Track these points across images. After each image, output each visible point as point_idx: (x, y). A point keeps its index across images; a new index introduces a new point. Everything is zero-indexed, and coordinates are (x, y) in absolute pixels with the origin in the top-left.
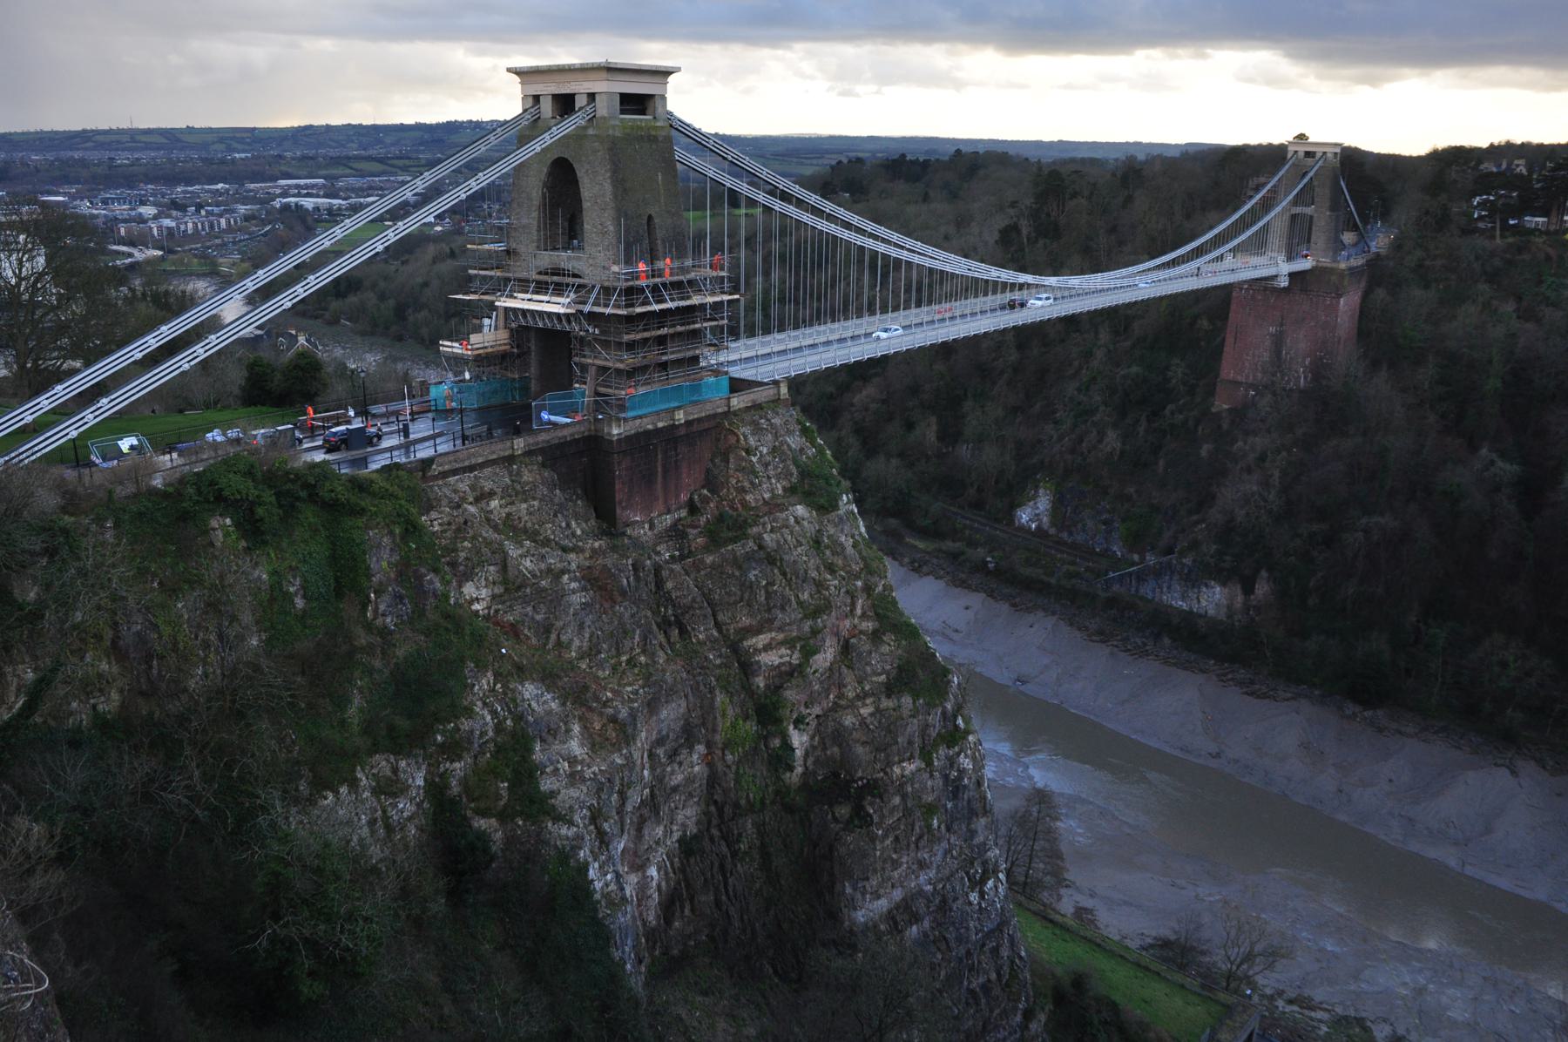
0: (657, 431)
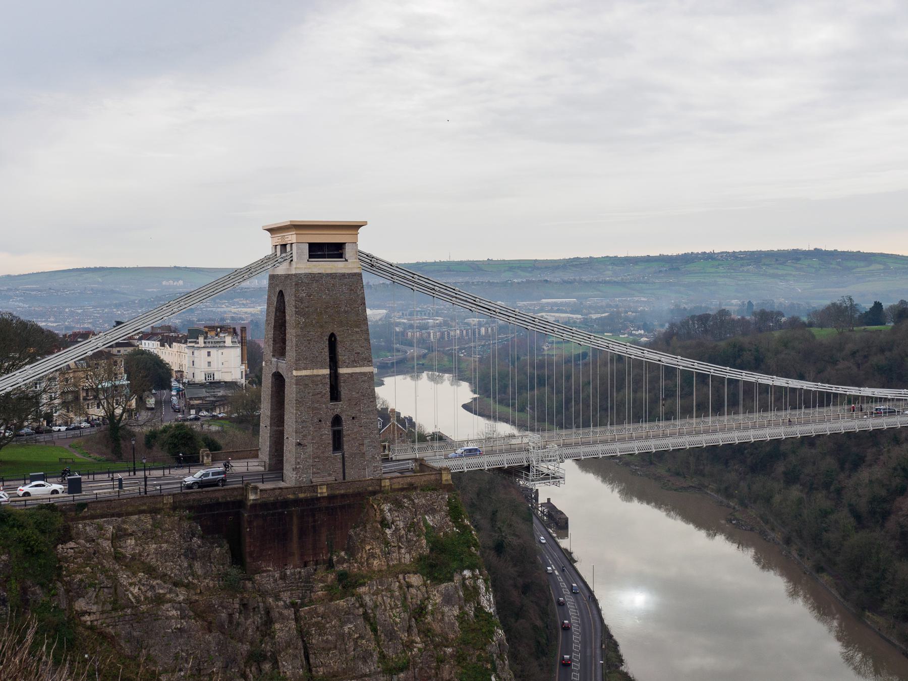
0: (297, 502)
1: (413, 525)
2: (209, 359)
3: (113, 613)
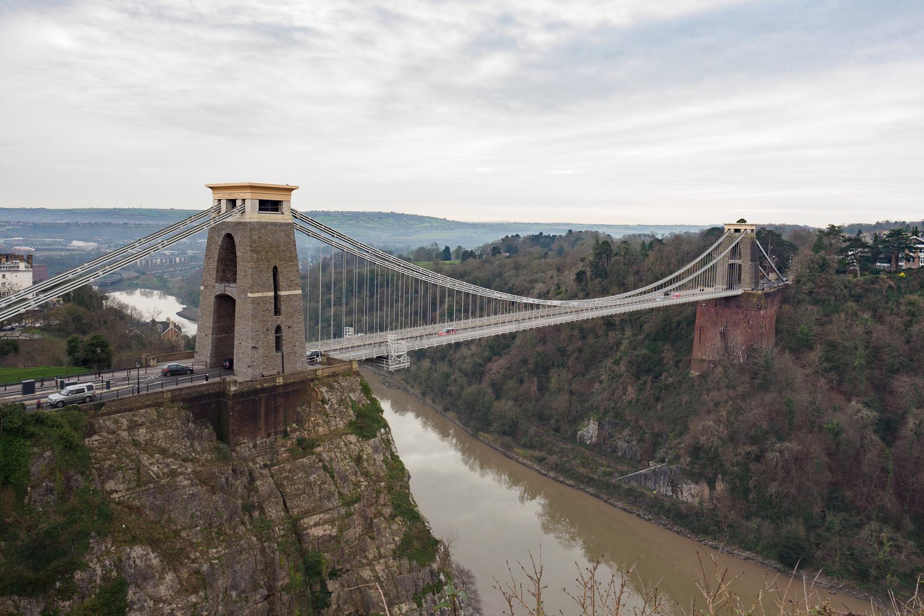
0: (263, 390)
1: (342, 400)
3: (137, 489)
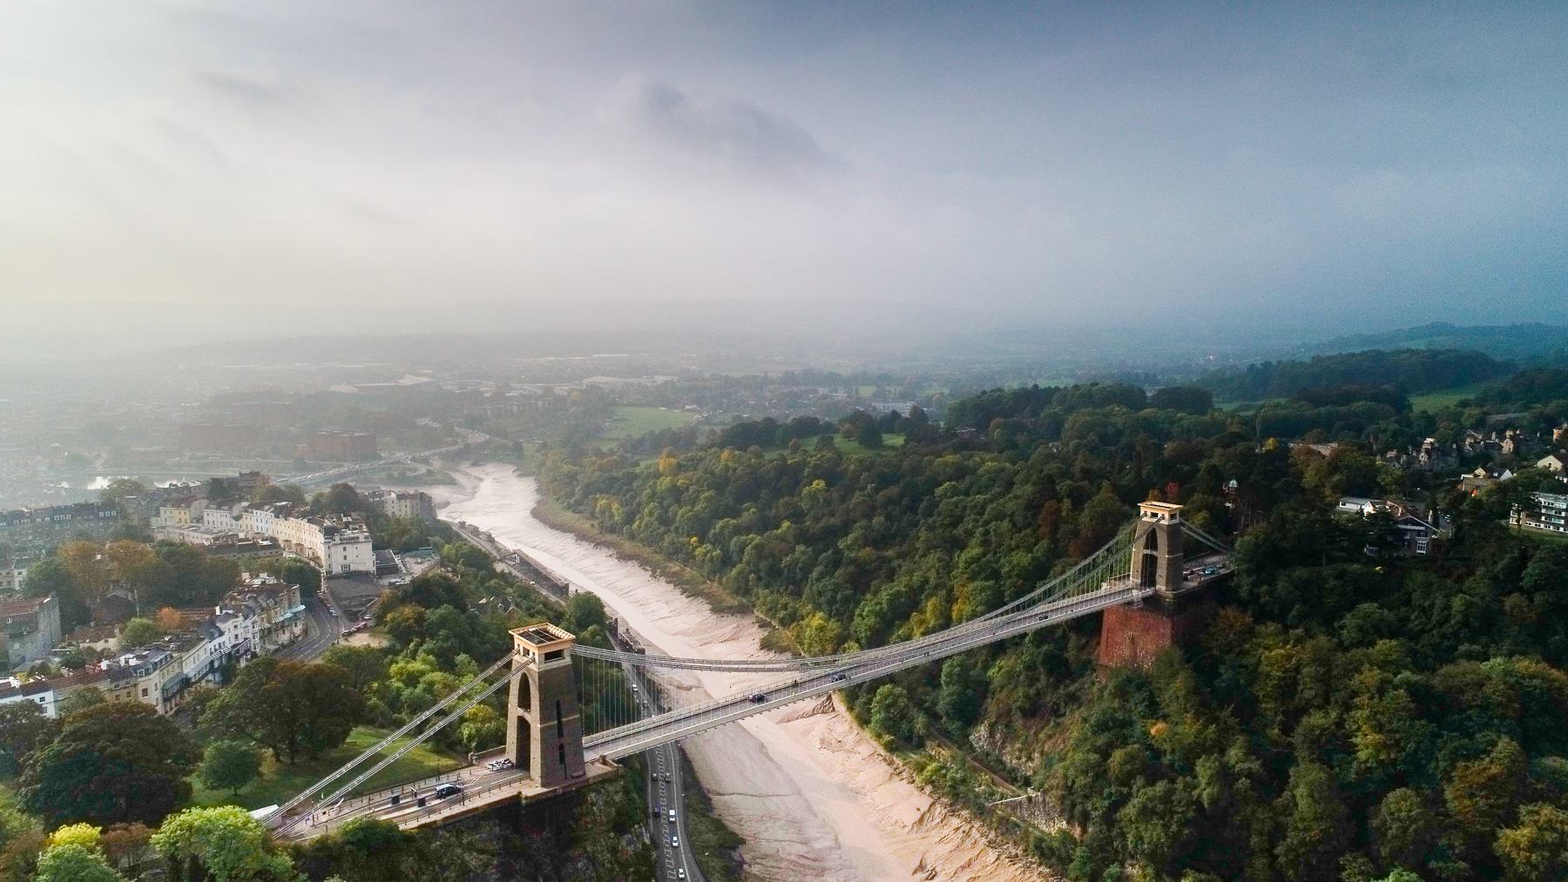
2: (345, 554)
